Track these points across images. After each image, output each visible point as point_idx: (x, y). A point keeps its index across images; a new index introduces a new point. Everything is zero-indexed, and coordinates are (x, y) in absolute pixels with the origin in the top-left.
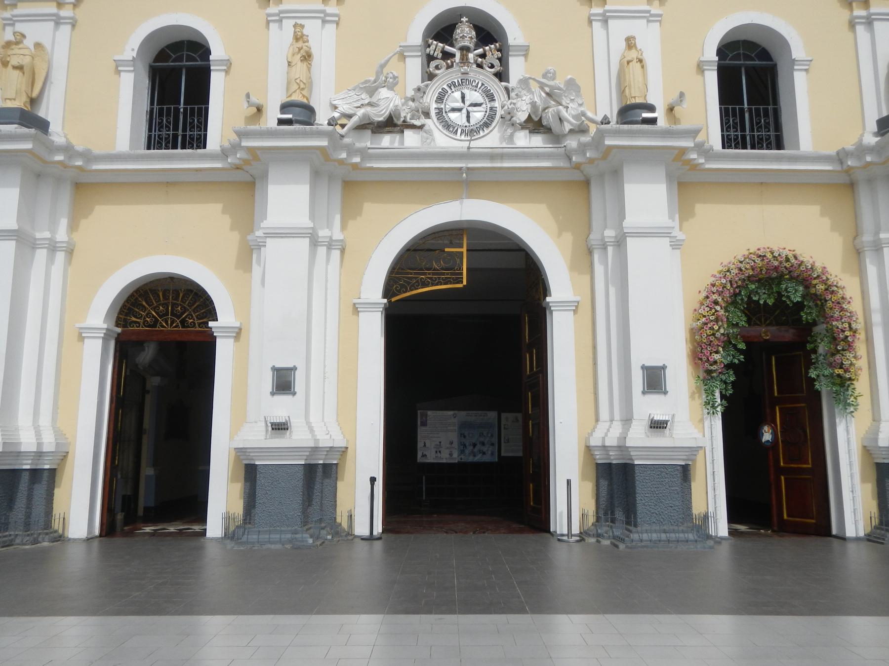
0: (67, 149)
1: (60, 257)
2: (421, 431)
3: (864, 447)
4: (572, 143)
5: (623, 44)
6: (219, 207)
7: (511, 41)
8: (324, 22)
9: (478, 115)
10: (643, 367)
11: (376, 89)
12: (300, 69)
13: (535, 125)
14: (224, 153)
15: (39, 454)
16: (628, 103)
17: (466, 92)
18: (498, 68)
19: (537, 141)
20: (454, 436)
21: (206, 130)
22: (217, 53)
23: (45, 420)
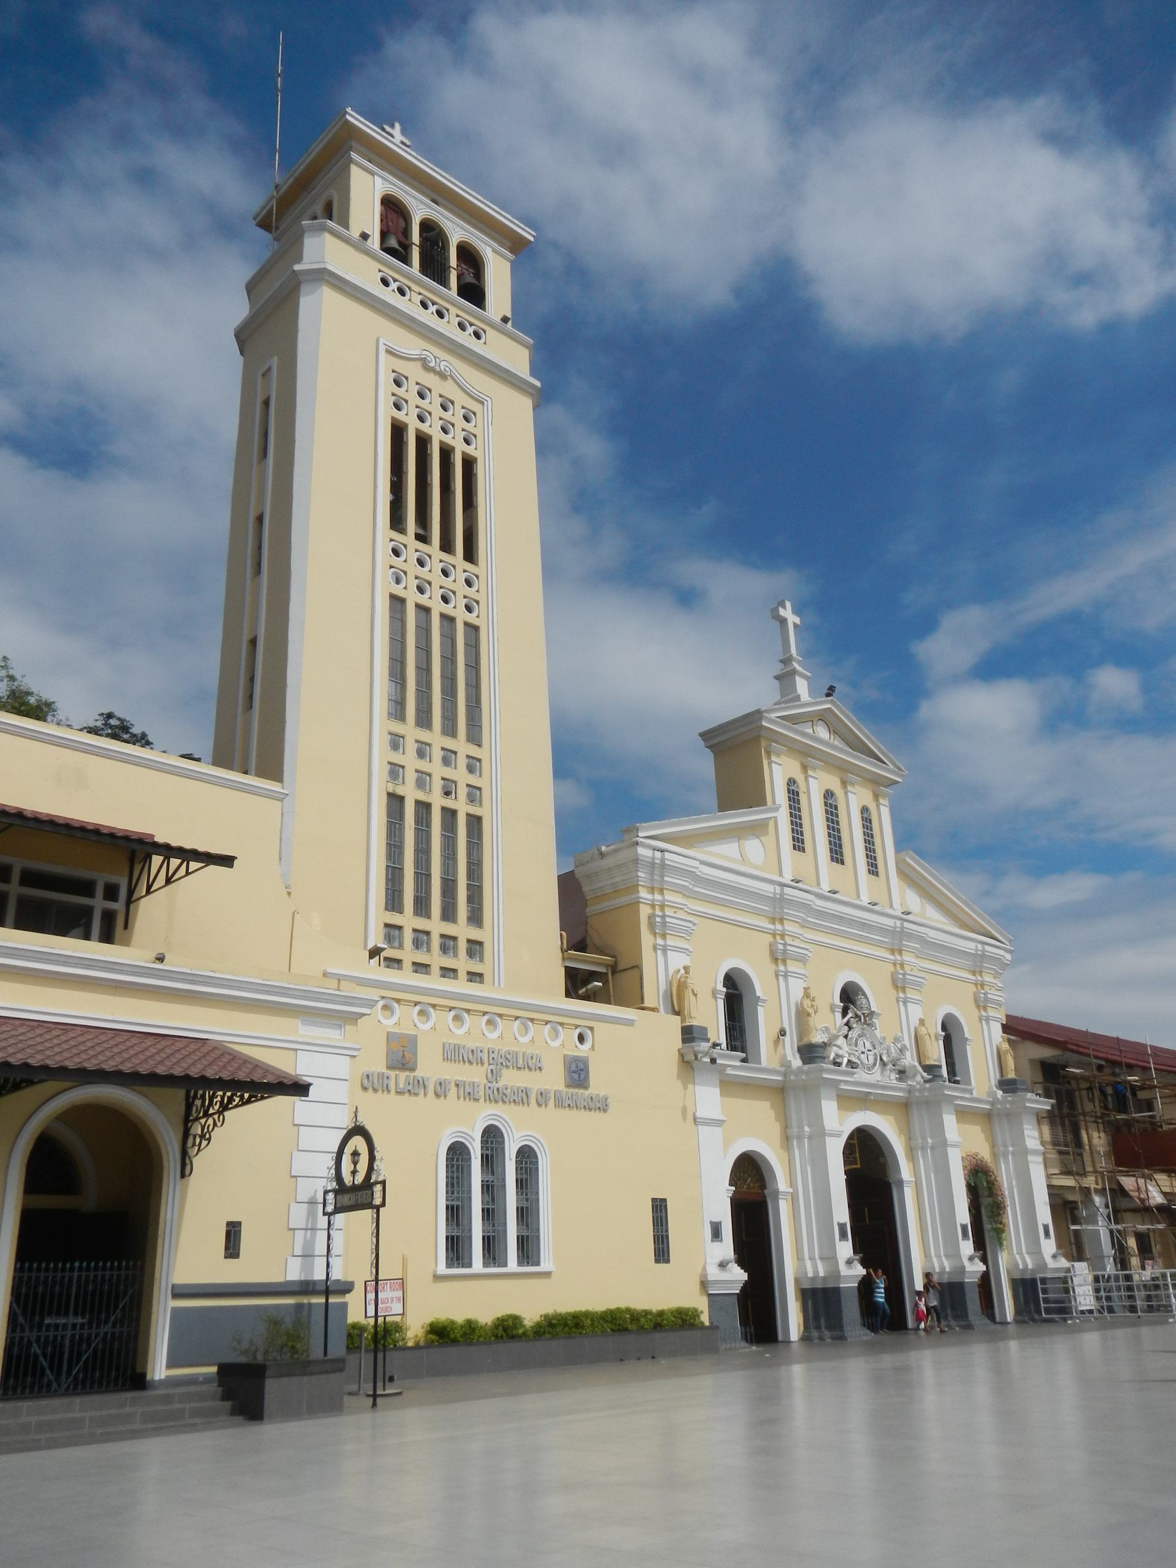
3: (1007, 1269)
5: (918, 1022)
6: (769, 1103)
9: (871, 1058)
10: (961, 1225)
11: (838, 1036)
16: (927, 1063)
17: (865, 1041)
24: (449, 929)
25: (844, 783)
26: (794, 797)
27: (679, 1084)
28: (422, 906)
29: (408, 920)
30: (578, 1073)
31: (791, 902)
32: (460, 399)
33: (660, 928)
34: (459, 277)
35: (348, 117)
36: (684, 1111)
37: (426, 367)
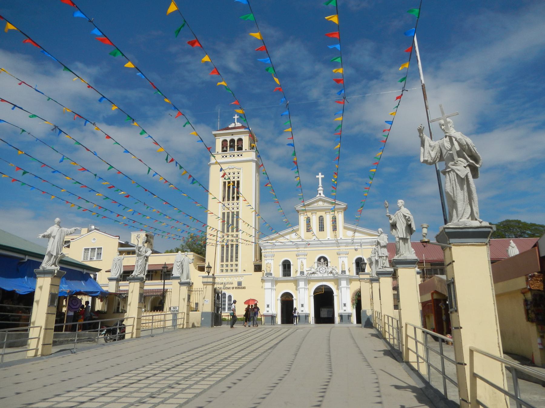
0: (276, 278)
1: (275, 290)
2: (321, 312)
4: (336, 275)
6: (293, 283)
7: (328, 261)
8: (305, 259)
9: (324, 271)
12: (302, 266)
13: (331, 272)
14: (294, 278)
15: (275, 314)
18: (327, 265)
19: (331, 275)
20: (326, 313)
21: (290, 272)
22: (291, 263)
23: (275, 310)
24: (232, 263)
25: (326, 213)
26: (308, 221)
27: (261, 283)
28: (227, 261)
29: (225, 263)
30: (240, 284)
31: (300, 245)
32: (236, 171)
33: (265, 257)
34: (237, 146)
35: (213, 133)
36: (262, 287)
37: (230, 169)
